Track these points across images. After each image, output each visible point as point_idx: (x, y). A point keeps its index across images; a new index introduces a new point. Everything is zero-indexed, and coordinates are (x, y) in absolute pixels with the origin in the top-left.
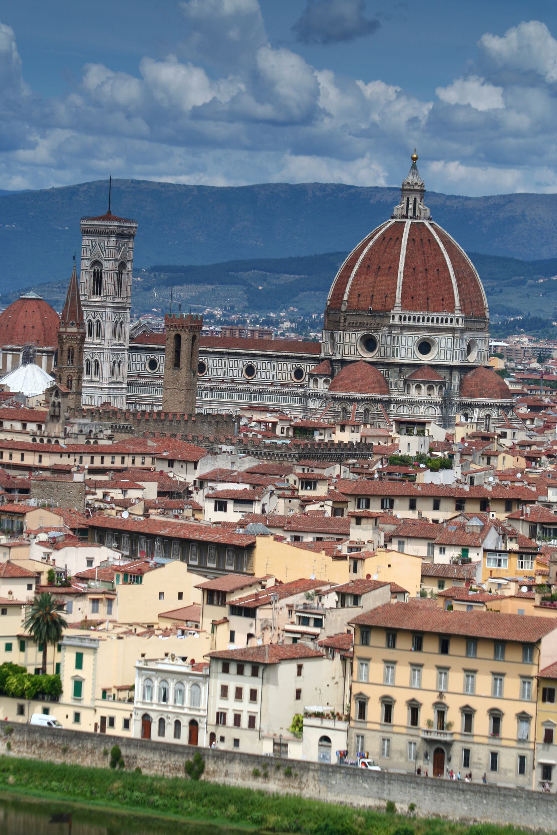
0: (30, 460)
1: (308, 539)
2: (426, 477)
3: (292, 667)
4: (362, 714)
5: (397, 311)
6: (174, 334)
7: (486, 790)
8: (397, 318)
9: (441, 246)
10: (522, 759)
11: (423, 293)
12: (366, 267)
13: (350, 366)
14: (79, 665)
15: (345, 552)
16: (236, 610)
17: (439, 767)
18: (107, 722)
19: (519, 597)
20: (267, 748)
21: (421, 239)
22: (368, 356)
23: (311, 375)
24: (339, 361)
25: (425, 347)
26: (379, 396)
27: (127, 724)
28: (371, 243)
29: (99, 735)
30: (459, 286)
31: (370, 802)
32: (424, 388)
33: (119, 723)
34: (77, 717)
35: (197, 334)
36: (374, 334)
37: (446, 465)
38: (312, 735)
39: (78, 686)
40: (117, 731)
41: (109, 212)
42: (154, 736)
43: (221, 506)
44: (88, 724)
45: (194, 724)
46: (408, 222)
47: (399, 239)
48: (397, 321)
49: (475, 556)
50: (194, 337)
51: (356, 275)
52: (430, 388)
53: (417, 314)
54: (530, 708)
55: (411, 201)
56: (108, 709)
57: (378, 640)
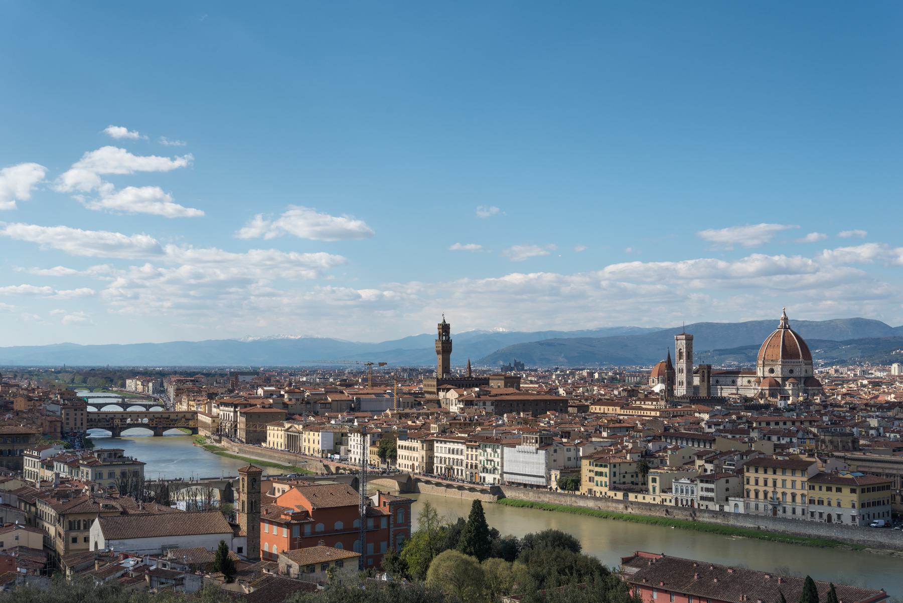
0: (653, 413)
1: (738, 436)
2: (787, 414)
3: (723, 480)
4: (748, 496)
7: (794, 521)
10: (803, 510)
14: (654, 480)
15: (747, 440)
16: (706, 462)
17: (775, 513)
18: (664, 500)
19: (801, 453)
20: (717, 508)
22: (772, 375)
25: (791, 371)
27: (670, 501)
29: (662, 505)
31: (752, 526)
33: (668, 501)
34: (654, 499)
37: (792, 410)
38: (732, 503)
39: (654, 489)
40: (668, 503)
42: (680, 505)
43: (710, 427)
44: (658, 501)
45: (692, 500)
49: (795, 440)
54: (805, 492)
56: (664, 496)
57: (752, 470)
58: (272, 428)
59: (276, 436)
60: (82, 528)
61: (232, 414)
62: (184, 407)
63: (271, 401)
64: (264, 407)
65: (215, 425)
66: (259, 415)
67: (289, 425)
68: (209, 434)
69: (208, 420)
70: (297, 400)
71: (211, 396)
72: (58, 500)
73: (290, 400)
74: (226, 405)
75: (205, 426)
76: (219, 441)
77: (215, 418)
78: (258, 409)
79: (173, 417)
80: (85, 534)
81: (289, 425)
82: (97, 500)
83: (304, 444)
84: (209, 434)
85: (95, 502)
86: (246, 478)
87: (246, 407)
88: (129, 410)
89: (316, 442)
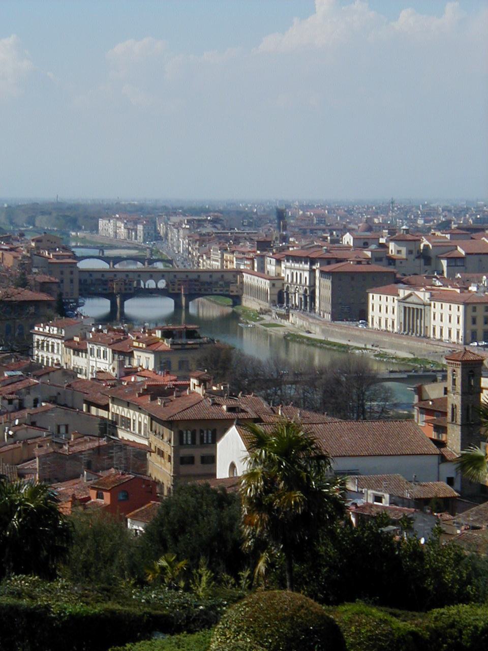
58: (377, 296)
59: (383, 308)
60: (198, 441)
61: (306, 274)
62: (216, 265)
63: (369, 254)
64: (359, 263)
65: (276, 291)
66: (352, 275)
67: (407, 292)
68: (266, 305)
69: (265, 284)
70: (410, 252)
71: (264, 245)
72: (154, 399)
73: (399, 252)
74: (296, 259)
75: (257, 292)
76: (286, 317)
77: (276, 280)
78: (350, 266)
79: (205, 278)
80: (206, 451)
81: (407, 292)
82: (217, 399)
83: (437, 323)
84: (266, 305)
85: (214, 404)
86: (459, 371)
87: (329, 263)
88: (117, 266)
89: (454, 319)
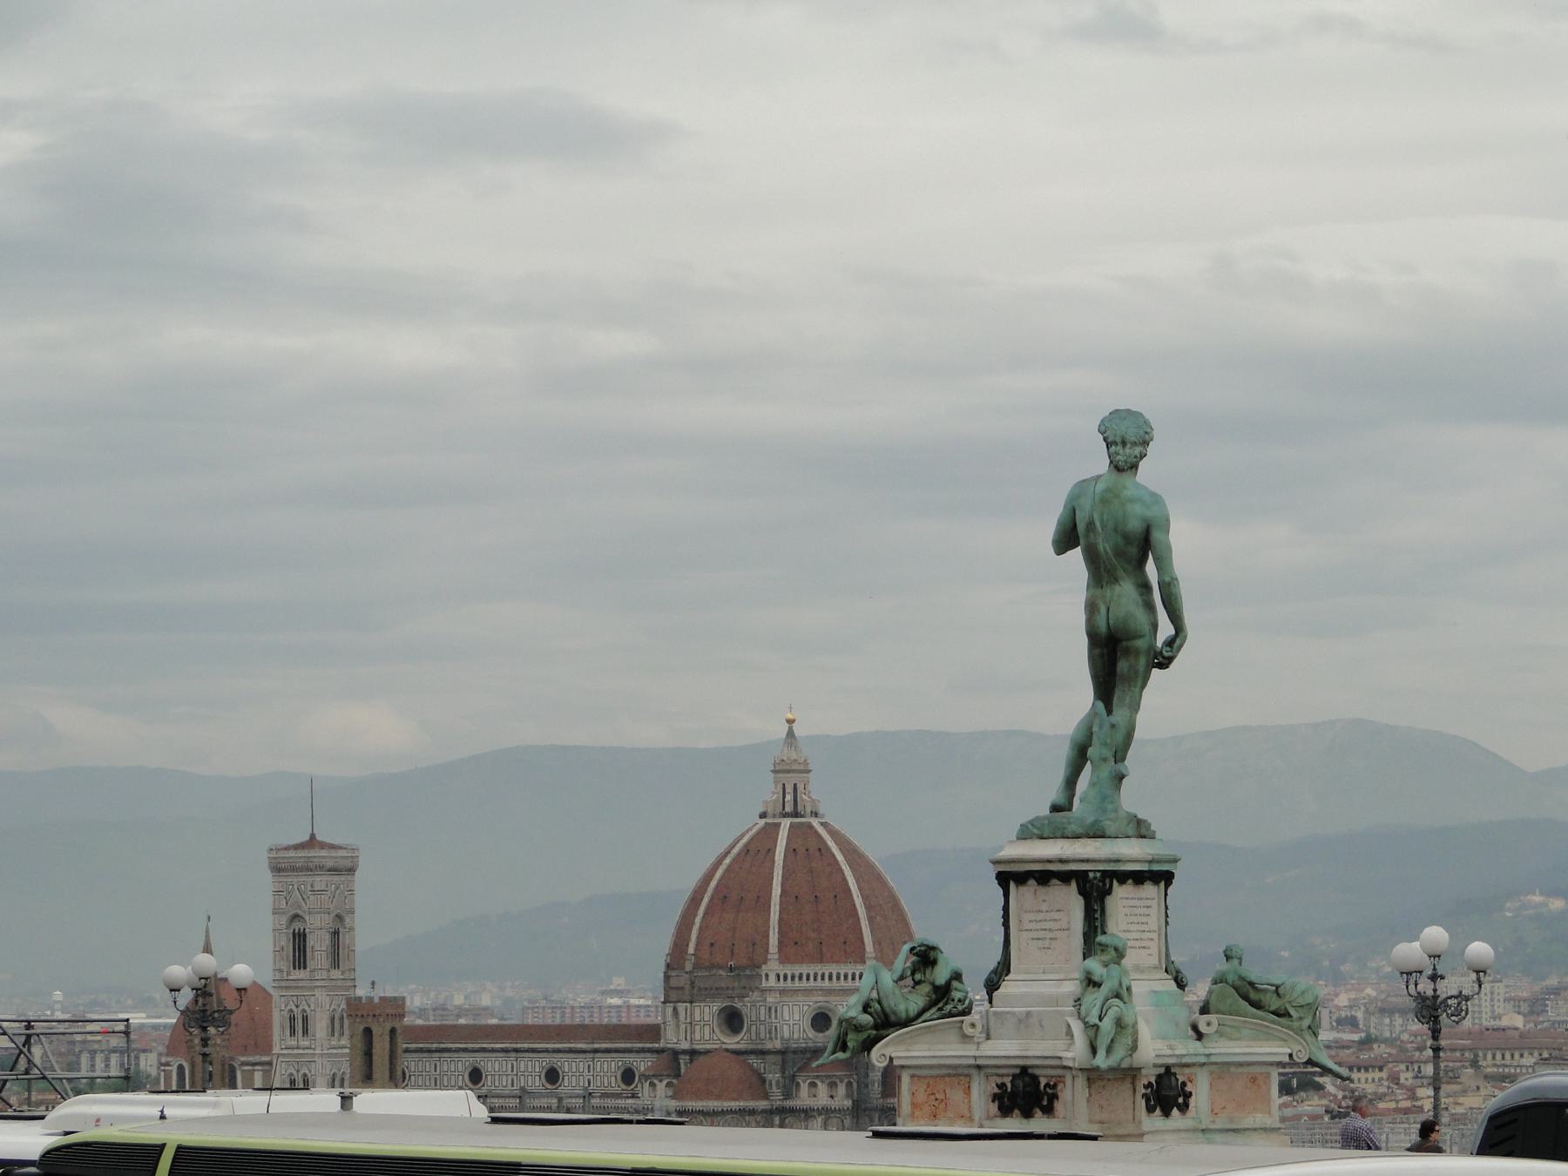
5: (773, 966)
6: (361, 1028)
8: (772, 977)
9: (840, 857)
11: (813, 935)
12: (722, 899)
13: (702, 1058)
21: (810, 851)
22: (732, 1042)
23: (644, 1077)
24: (684, 1052)
26: (751, 1104)
28: (727, 861)
30: (871, 920)
32: (822, 1089)
35: (397, 1026)
36: (738, 1005)
41: (313, 836)
46: (786, 823)
47: (771, 851)
48: (772, 982)
50: (393, 1031)
51: (706, 913)
52: (833, 1085)
53: (804, 969)
55: (789, 789)
